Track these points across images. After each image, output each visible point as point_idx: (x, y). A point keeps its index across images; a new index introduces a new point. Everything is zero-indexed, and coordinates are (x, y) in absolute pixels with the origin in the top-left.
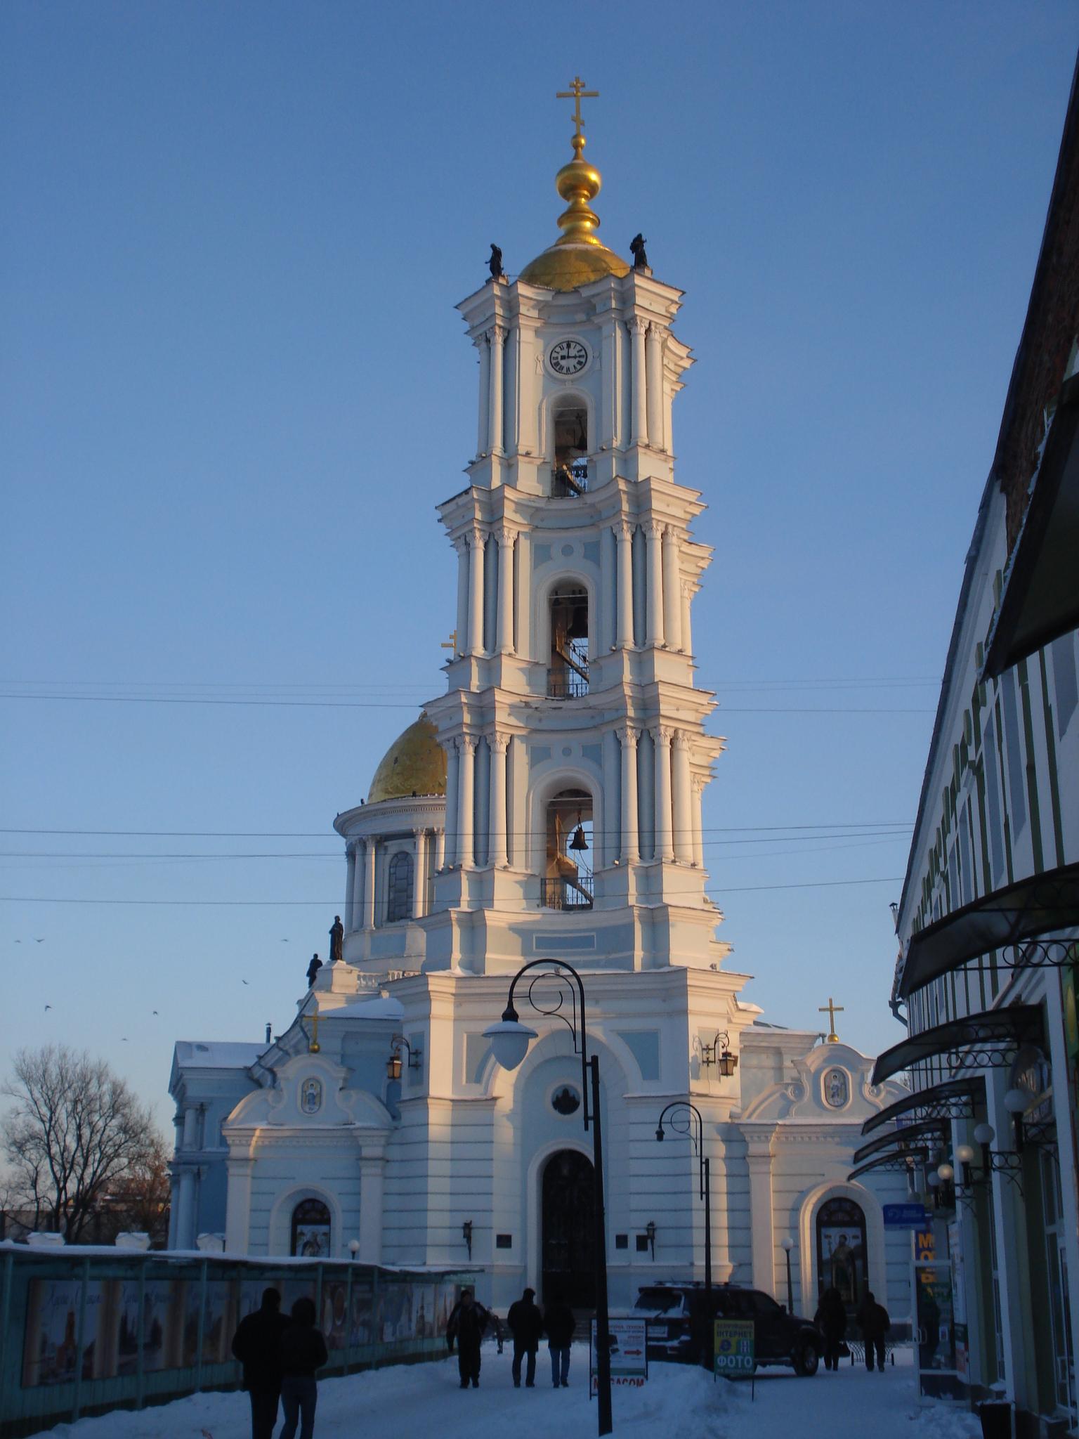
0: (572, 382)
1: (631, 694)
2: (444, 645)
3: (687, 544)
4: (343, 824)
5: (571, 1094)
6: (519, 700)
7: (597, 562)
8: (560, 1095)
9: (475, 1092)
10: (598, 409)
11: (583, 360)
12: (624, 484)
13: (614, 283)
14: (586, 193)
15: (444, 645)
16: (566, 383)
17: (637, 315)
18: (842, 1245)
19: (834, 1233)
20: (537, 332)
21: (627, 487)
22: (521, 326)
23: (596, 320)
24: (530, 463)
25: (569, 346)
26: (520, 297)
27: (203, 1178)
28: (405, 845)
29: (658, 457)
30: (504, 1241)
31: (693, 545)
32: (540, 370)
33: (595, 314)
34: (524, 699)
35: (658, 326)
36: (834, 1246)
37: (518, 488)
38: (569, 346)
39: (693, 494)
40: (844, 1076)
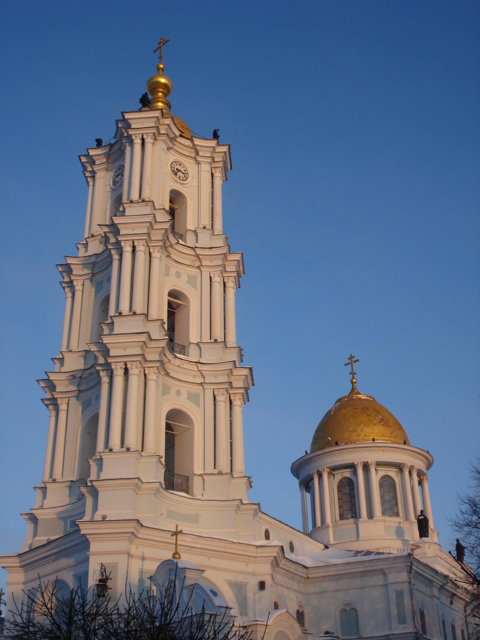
0: (120, 187)
1: (97, 349)
2: (346, 365)
3: (209, 249)
6: (68, 375)
12: (106, 228)
13: (120, 124)
14: (161, 90)
15: (346, 365)
16: (118, 190)
17: (131, 134)
20: (107, 170)
21: (109, 230)
22: (96, 171)
24: (94, 240)
26: (93, 157)
29: (138, 205)
31: (213, 249)
32: (108, 189)
34: (71, 374)
35: (148, 134)
39: (148, 217)
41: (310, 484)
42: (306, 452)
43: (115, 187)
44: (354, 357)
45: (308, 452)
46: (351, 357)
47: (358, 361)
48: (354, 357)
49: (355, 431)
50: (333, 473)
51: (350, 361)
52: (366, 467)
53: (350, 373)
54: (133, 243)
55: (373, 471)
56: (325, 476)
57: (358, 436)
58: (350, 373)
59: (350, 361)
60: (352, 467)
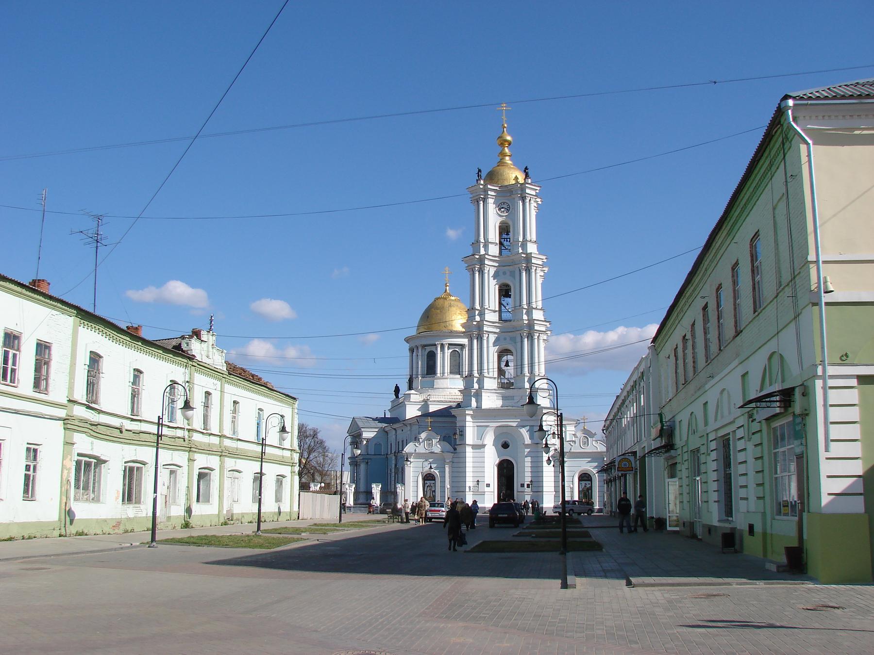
4: (407, 340)
5: (507, 443)
7: (514, 277)
8: (504, 443)
9: (479, 442)
10: (514, 225)
11: (509, 209)
18: (585, 486)
19: (583, 483)
23: (513, 196)
25: (504, 204)
27: (369, 464)
28: (433, 348)
30: (488, 485)
33: (513, 194)
36: (583, 487)
37: (489, 254)
38: (504, 204)
40: (588, 439)
56: (446, 348)
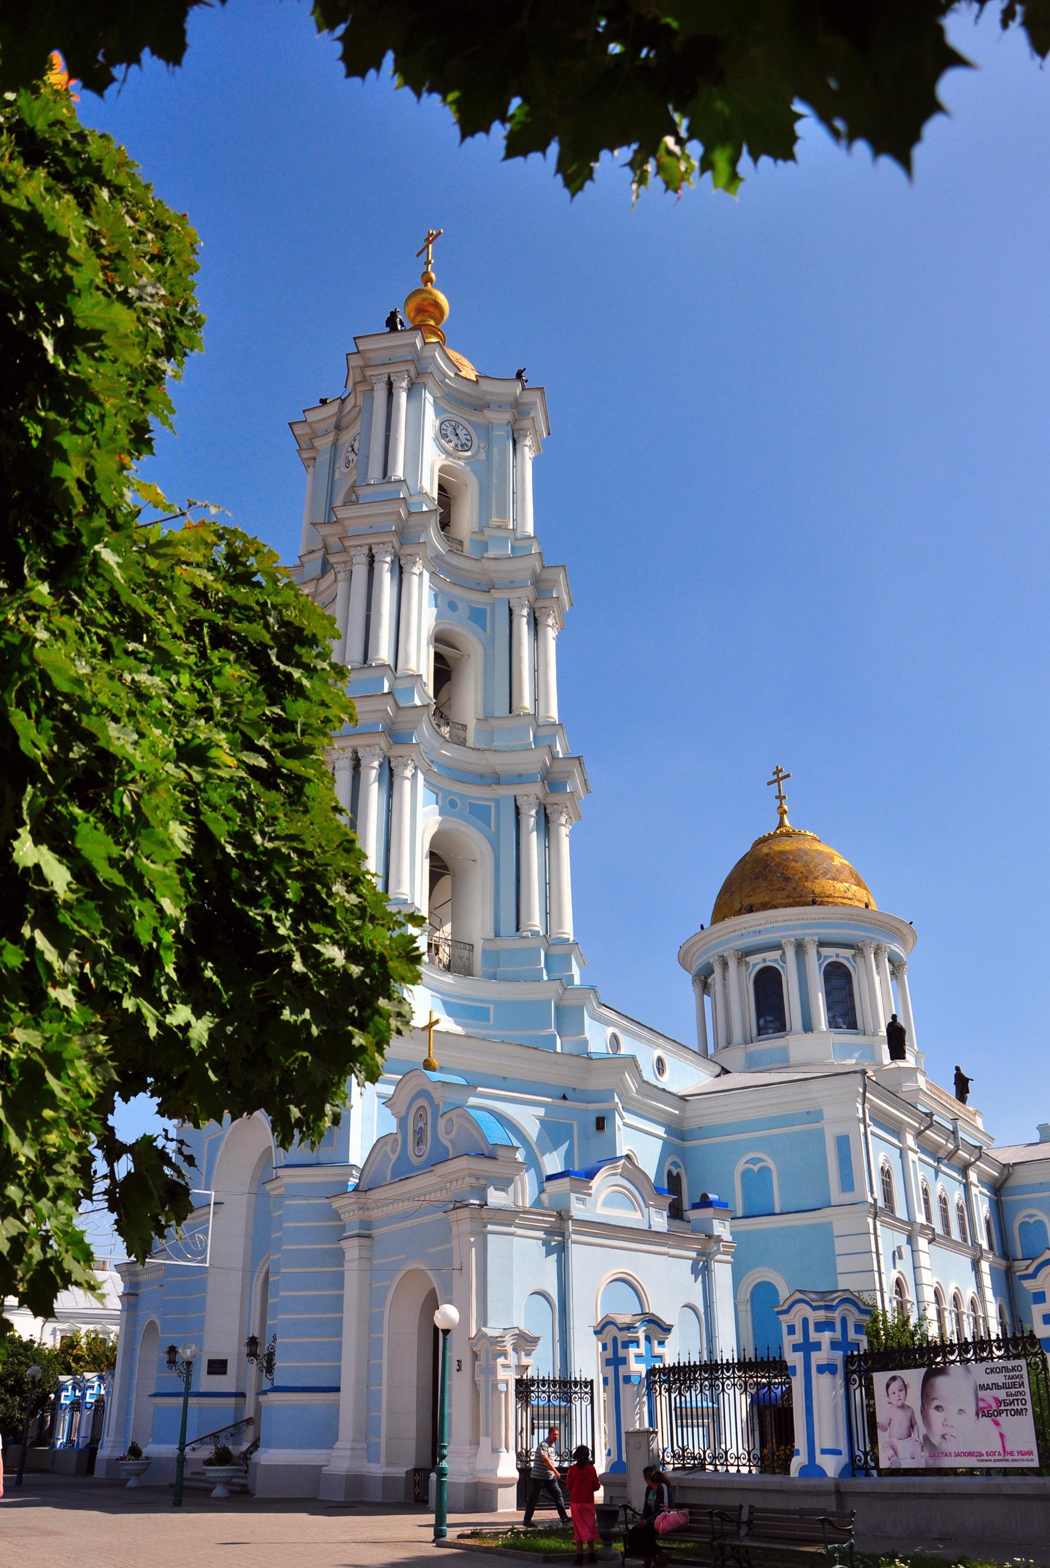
2: (769, 784)
15: (769, 784)
41: (709, 981)
42: (702, 927)
43: (347, 470)
44: (781, 771)
45: (706, 926)
46: (778, 771)
47: (788, 776)
48: (781, 771)
49: (783, 890)
50: (747, 959)
51: (775, 777)
52: (800, 948)
53: (777, 797)
54: (370, 550)
55: (812, 951)
56: (732, 964)
57: (788, 897)
58: (777, 797)
59: (775, 777)
60: (778, 947)
